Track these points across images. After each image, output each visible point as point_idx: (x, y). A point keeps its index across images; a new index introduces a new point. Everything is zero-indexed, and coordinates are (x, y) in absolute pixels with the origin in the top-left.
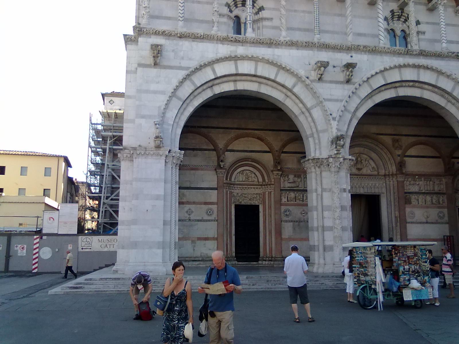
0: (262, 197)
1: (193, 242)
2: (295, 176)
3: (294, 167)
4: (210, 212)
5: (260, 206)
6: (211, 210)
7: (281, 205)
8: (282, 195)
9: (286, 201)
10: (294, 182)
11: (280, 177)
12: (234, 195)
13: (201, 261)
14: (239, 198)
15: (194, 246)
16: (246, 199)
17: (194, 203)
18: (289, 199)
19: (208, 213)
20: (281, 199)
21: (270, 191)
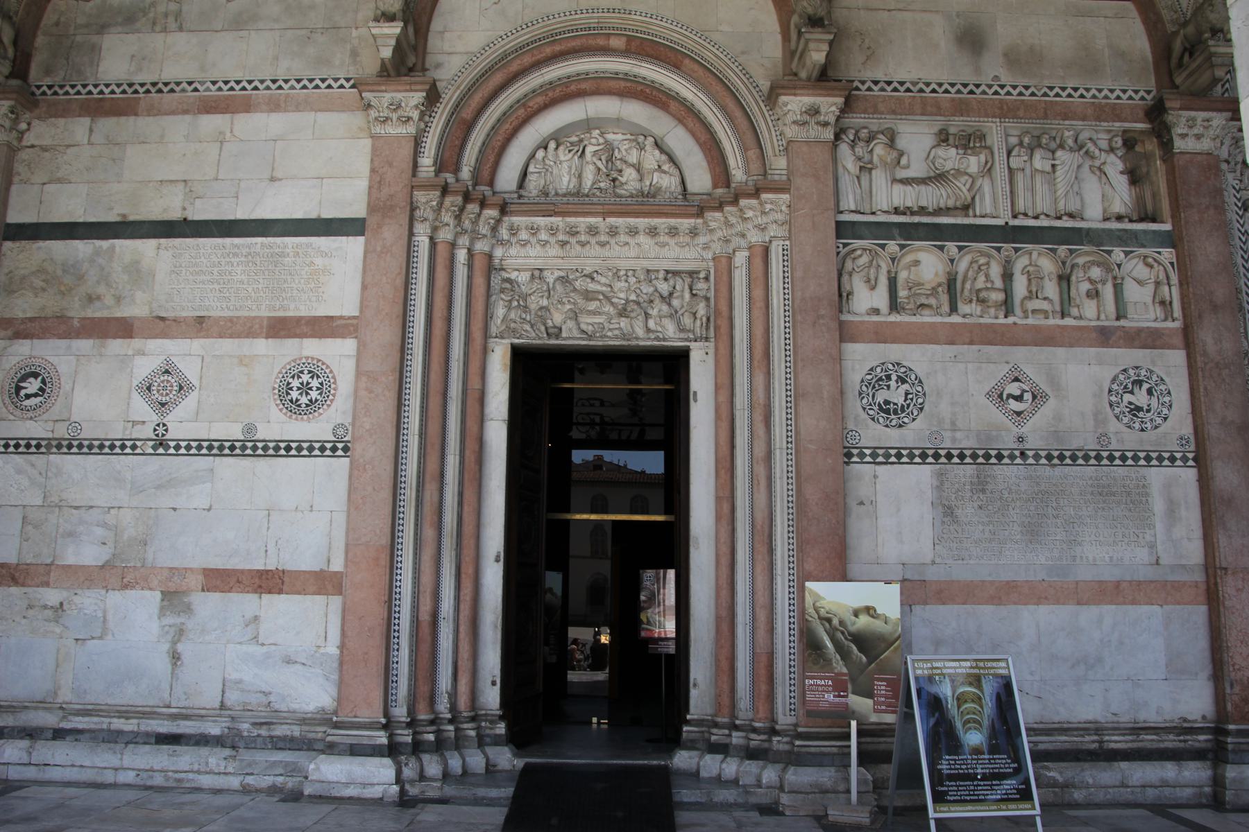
0: (712, 294)
1: (173, 599)
2: (943, 138)
3: (926, 76)
4: (305, 388)
5: (696, 357)
6: (313, 375)
7: (845, 333)
8: (849, 265)
9: (880, 298)
10: (939, 178)
11: (829, 134)
12: (508, 280)
13: (218, 741)
14: (545, 302)
15: (180, 632)
16: (593, 306)
17: (200, 326)
18: (902, 293)
19: (294, 394)
20: (843, 297)
21: (755, 237)
